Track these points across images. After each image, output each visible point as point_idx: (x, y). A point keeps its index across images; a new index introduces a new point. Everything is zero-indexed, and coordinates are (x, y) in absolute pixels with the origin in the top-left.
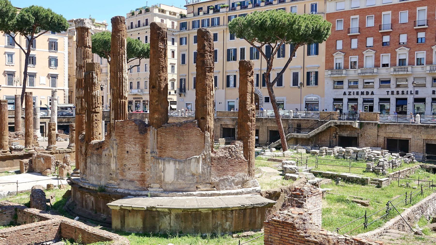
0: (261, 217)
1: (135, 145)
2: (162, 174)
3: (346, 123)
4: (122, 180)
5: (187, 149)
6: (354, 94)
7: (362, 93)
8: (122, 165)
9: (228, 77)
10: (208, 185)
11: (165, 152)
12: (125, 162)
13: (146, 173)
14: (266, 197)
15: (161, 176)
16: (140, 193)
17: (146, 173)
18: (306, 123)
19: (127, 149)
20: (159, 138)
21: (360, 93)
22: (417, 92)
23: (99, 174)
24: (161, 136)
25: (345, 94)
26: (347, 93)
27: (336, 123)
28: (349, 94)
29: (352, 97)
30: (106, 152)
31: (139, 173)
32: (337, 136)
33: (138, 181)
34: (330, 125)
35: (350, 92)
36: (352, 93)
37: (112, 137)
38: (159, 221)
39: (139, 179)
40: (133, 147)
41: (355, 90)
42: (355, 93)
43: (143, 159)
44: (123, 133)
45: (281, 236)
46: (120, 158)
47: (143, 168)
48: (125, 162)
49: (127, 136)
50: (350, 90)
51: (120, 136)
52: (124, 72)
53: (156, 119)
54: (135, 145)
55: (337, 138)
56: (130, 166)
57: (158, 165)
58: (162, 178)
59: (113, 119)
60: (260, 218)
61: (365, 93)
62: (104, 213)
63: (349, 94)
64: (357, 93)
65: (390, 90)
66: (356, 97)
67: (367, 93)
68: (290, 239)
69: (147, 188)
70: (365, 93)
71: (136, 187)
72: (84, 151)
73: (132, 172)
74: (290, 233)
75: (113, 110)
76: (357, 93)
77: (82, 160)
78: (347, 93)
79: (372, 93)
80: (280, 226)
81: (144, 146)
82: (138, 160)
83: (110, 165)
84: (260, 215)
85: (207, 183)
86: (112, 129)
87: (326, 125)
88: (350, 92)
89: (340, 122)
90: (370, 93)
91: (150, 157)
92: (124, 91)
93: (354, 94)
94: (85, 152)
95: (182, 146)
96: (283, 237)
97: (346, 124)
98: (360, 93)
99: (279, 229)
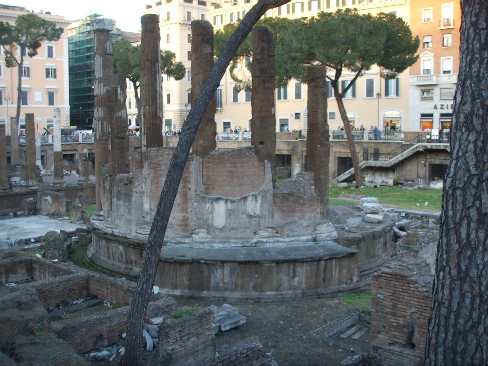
0: (339, 271)
2: (210, 216)
3: (439, 146)
5: (242, 184)
6: (447, 108)
9: (397, 94)
10: (270, 230)
11: (213, 188)
13: (188, 215)
14: (344, 245)
15: (208, 219)
16: (183, 240)
17: (188, 215)
20: (205, 170)
23: (128, 217)
24: (207, 167)
25: (435, 107)
26: (439, 107)
27: (425, 146)
28: (442, 108)
30: (138, 190)
32: (427, 163)
33: (179, 225)
34: (418, 149)
35: (442, 105)
36: (445, 107)
37: (144, 169)
38: (209, 276)
39: (180, 223)
44: (158, 164)
45: (394, 291)
50: (442, 103)
52: (158, 86)
53: (200, 145)
55: (427, 166)
57: (204, 206)
58: (210, 221)
59: (145, 146)
60: (337, 271)
62: (136, 266)
63: (442, 108)
68: (406, 294)
69: (191, 234)
71: (176, 234)
72: (108, 188)
74: (404, 288)
75: (144, 134)
77: (105, 199)
78: (439, 107)
80: (393, 279)
83: (143, 206)
84: (337, 268)
85: (268, 227)
86: (143, 160)
87: (413, 150)
88: (442, 105)
89: (432, 146)
91: (193, 195)
92: (158, 110)
93: (447, 108)
94: (110, 189)
95: (235, 180)
96: (396, 292)
97: (439, 148)
99: (392, 282)
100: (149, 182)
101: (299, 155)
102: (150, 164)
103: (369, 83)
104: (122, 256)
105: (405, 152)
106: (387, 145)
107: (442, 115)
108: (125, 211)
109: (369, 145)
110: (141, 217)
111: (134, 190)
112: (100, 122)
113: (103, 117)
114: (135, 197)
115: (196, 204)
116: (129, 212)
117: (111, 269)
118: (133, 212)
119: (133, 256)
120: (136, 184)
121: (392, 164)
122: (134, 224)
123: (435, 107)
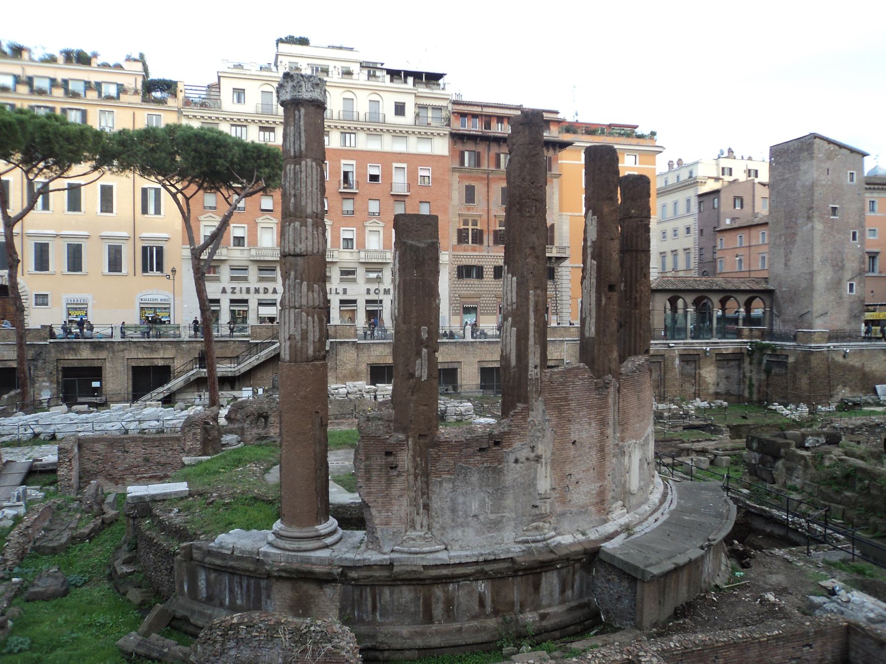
1: (590, 424)
4: (563, 514)
7: (257, 291)
8: (562, 479)
12: (568, 469)
18: (222, 348)
19: (574, 437)
21: (252, 290)
22: (345, 291)
23: (492, 517)
25: (224, 291)
26: (229, 290)
28: (233, 292)
29: (237, 296)
31: (595, 487)
36: (237, 290)
39: (595, 501)
40: (584, 430)
41: (244, 285)
42: (244, 291)
43: (602, 450)
44: (566, 399)
46: (558, 463)
47: (601, 476)
48: (568, 469)
49: (573, 405)
50: (234, 284)
51: (558, 409)
54: (590, 424)
56: (581, 475)
61: (262, 291)
63: (233, 292)
64: (248, 291)
65: (382, 288)
66: (245, 296)
67: (266, 291)
70: (262, 291)
73: (584, 488)
76: (248, 291)
78: (229, 290)
79: (275, 291)
81: (603, 423)
82: (593, 457)
88: (234, 288)
90: (271, 290)
98: (252, 290)
100: (549, 434)
101: (51, 367)
102: (546, 402)
103: (113, 251)
104: (482, 603)
105: (263, 353)
106: (223, 344)
107: (232, 301)
108: (483, 505)
109: (191, 345)
110: (529, 508)
111: (512, 458)
112: (316, 316)
113: (322, 305)
114: (513, 473)
115: (614, 460)
116: (498, 507)
117: (461, 642)
118: (509, 502)
119: (515, 592)
120: (517, 444)
121: (242, 371)
122: (510, 528)
123: (224, 291)
